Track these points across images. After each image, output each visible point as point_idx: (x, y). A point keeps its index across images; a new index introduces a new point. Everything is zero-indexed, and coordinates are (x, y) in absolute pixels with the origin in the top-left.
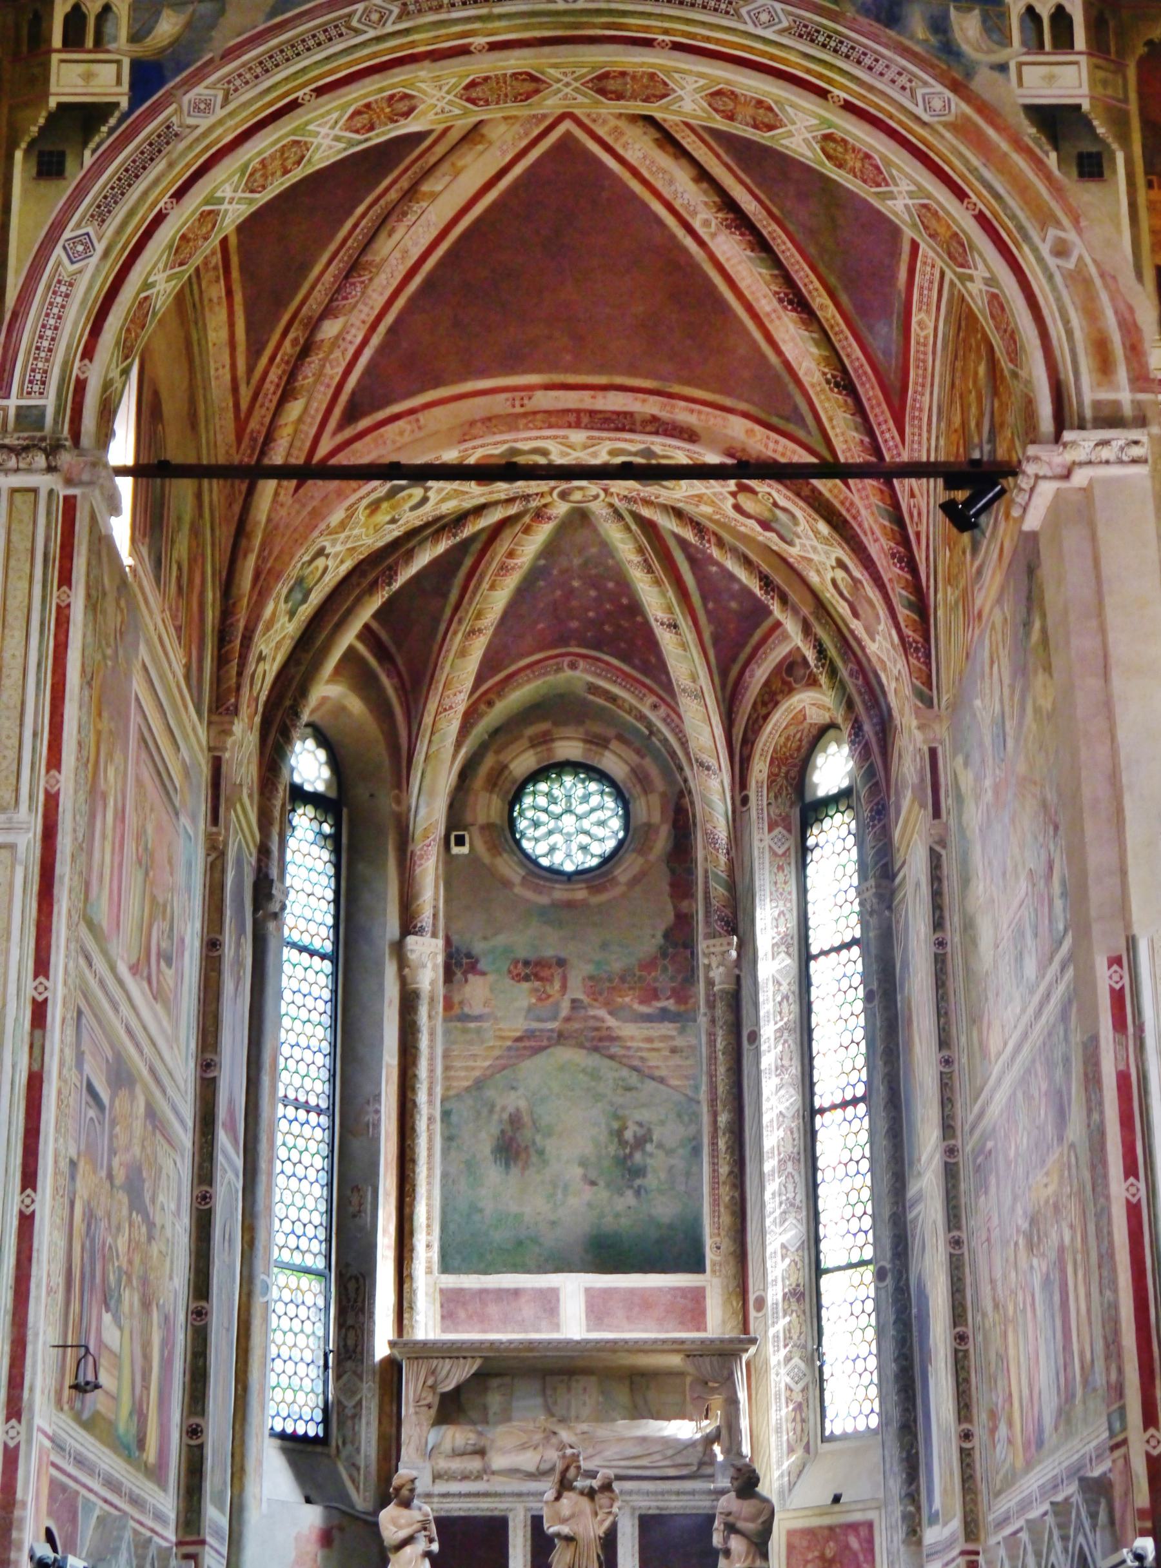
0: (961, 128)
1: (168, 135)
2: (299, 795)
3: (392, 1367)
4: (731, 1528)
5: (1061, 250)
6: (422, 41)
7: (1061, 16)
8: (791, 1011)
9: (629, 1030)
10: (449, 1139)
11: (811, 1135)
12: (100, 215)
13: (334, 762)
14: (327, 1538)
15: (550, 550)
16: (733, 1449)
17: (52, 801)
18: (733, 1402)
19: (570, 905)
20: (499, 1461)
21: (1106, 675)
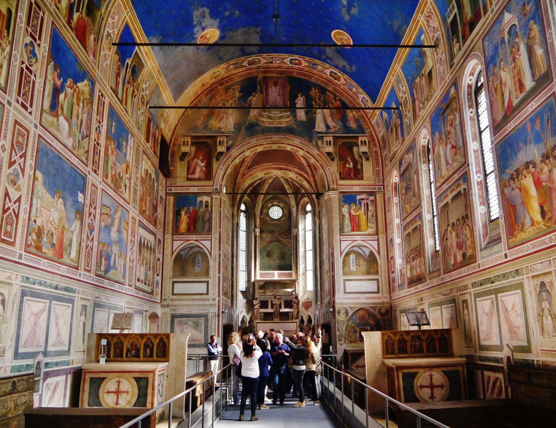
0: (319, 155)
1: (231, 156)
2: (242, 211)
3: (254, 282)
4: (294, 303)
5: (329, 170)
6: (259, 144)
7: (330, 141)
8: (303, 238)
9: (283, 240)
10: (261, 254)
11: (306, 254)
12: (223, 165)
13: (246, 206)
14: (247, 303)
15: (273, 180)
16: (295, 293)
17: (220, 232)
18: (295, 287)
19: (276, 224)
20: (267, 294)
21: (332, 218)
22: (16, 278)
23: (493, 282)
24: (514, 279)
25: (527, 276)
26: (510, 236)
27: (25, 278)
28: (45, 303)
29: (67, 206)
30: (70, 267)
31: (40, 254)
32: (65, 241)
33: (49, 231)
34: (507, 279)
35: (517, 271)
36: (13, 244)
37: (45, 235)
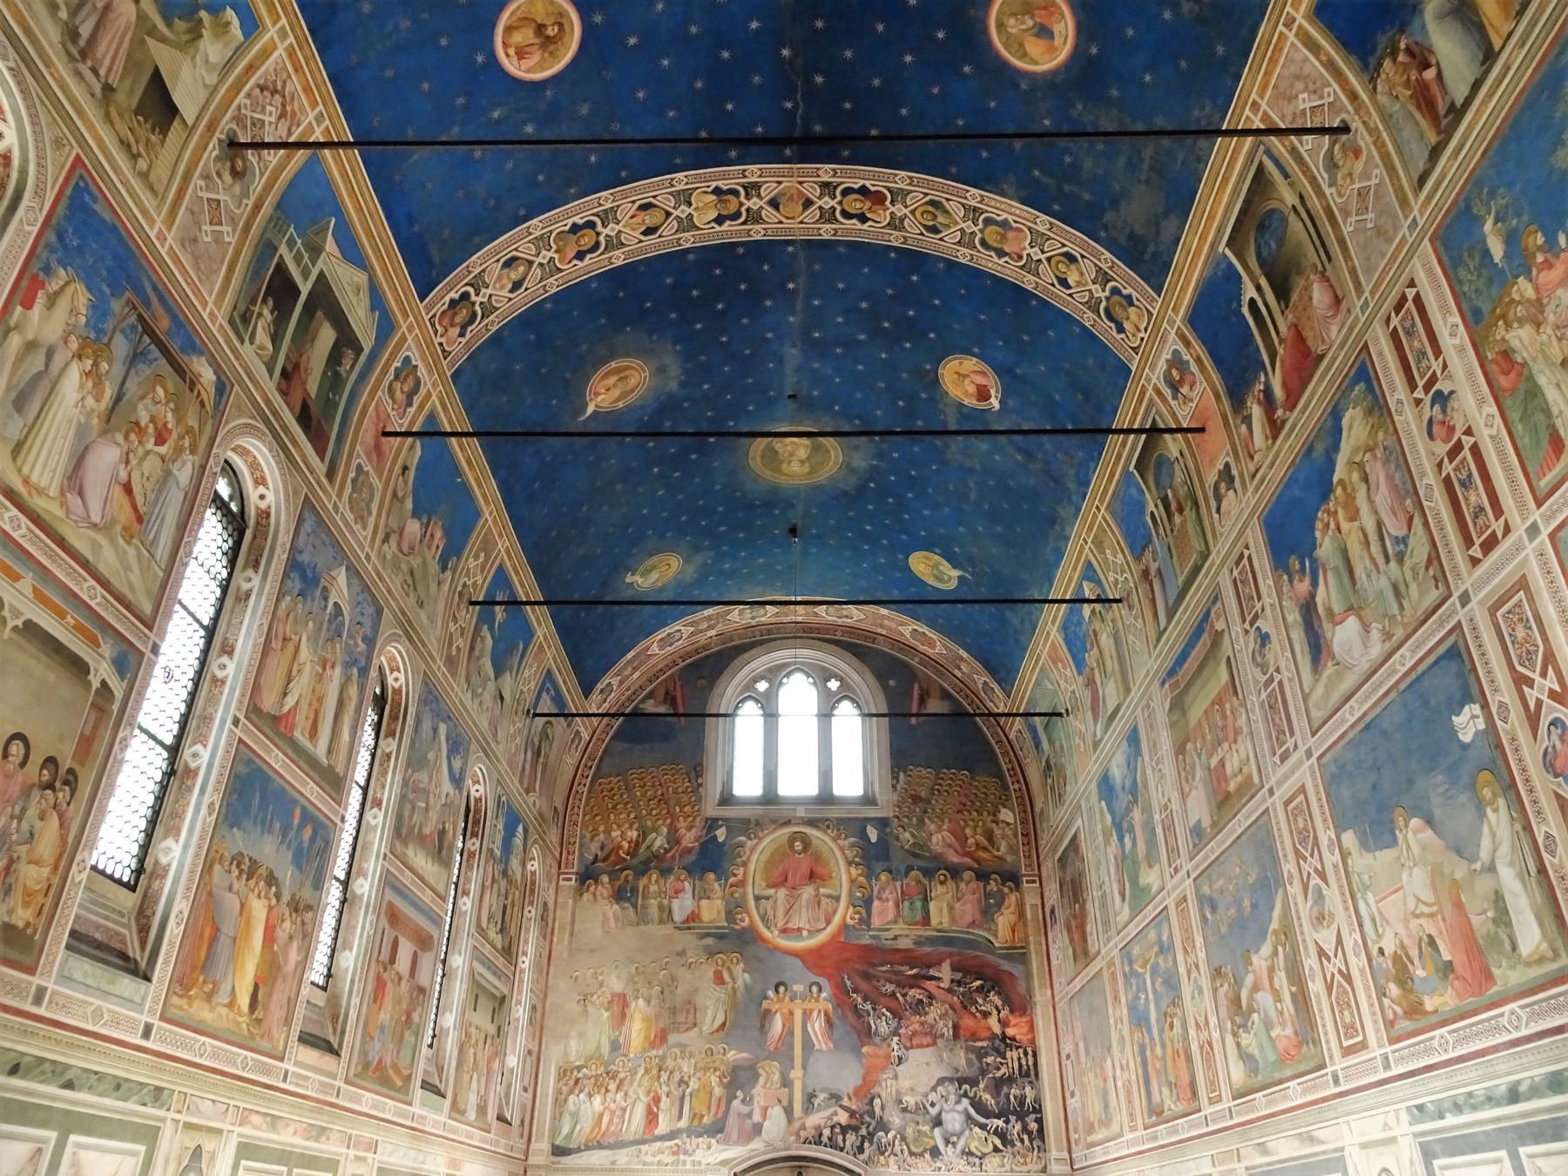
22: (1397, 1118)
23: (69, 1085)
24: (143, 1109)
25: (177, 1116)
26: (178, 989)
27: (1415, 1111)
28: (1498, 1161)
29: (1438, 813)
30: (1533, 991)
31: (1422, 1023)
32: (1476, 921)
33: (1421, 940)
34: (125, 1100)
35: (159, 1090)
36: (1363, 1046)
37: (1416, 961)
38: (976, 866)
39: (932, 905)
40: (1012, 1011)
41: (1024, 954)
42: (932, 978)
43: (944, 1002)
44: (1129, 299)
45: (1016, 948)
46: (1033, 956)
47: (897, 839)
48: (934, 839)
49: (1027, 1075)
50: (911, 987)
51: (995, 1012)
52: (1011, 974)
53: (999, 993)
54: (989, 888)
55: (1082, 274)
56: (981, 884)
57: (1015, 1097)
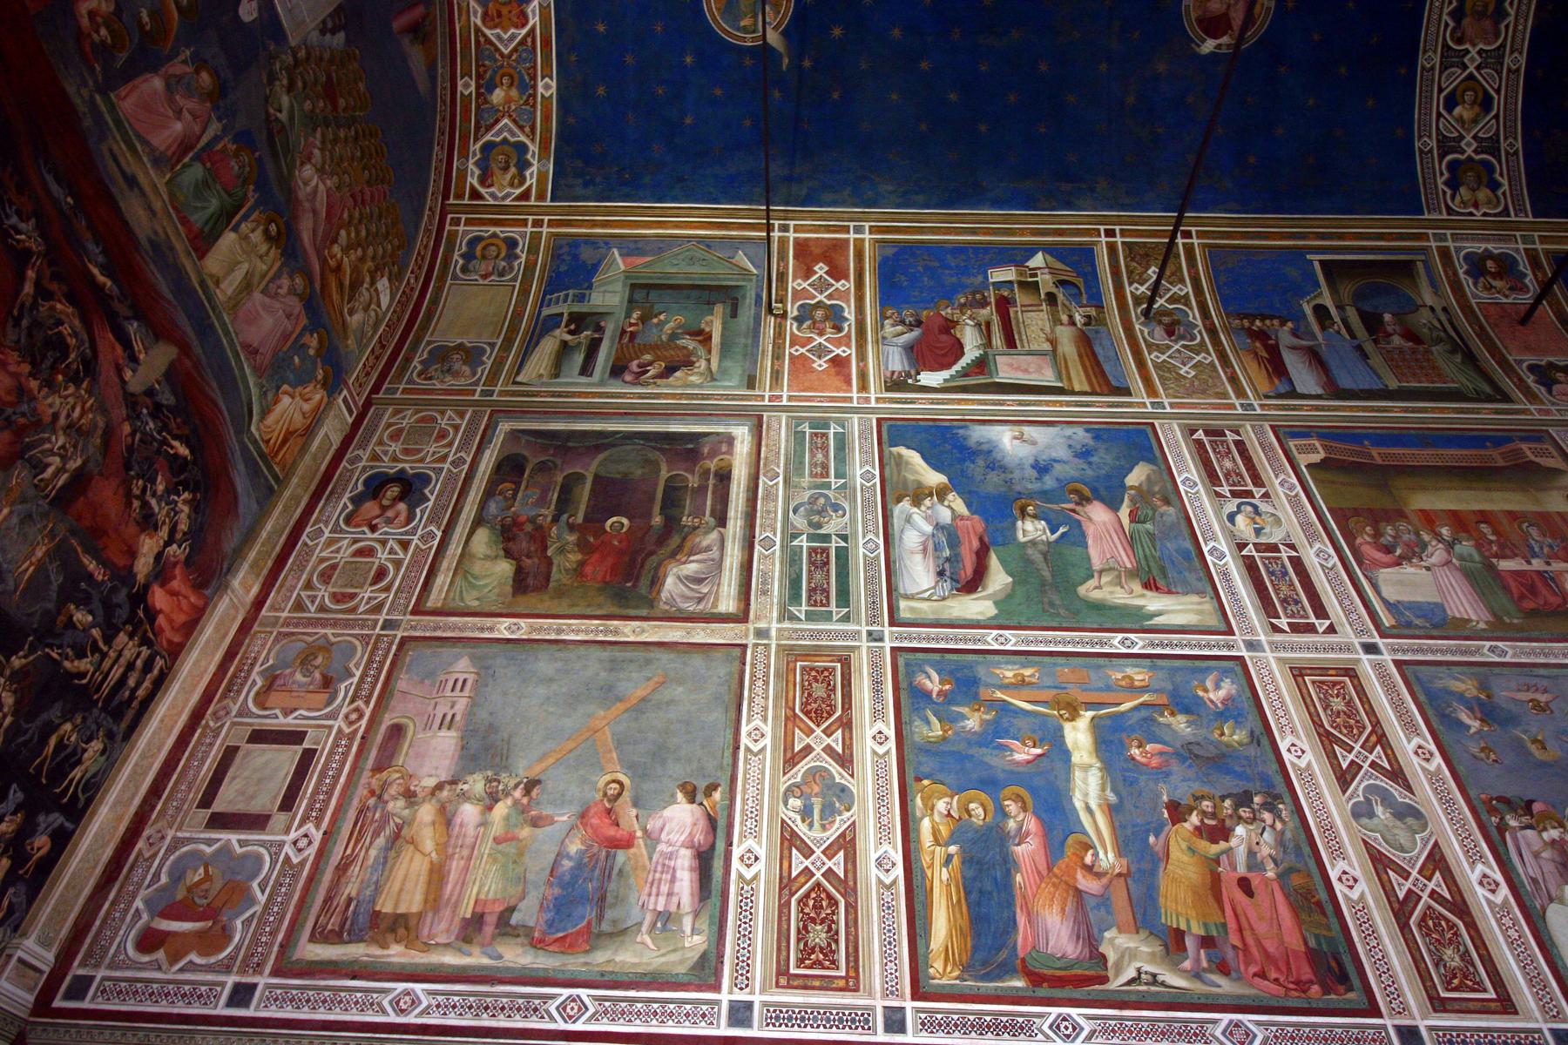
38: (318, 286)
39: (229, 239)
40: (188, 562)
41: (271, 489)
42: (127, 345)
43: (102, 409)
44: (1494, 186)
45: (270, 468)
46: (280, 507)
47: (272, 78)
48: (308, 171)
49: (117, 715)
50: (72, 299)
51: (164, 533)
52: (236, 498)
53: (195, 506)
54: (306, 339)
55: (1475, 121)
56: (304, 321)
57: (60, 745)
